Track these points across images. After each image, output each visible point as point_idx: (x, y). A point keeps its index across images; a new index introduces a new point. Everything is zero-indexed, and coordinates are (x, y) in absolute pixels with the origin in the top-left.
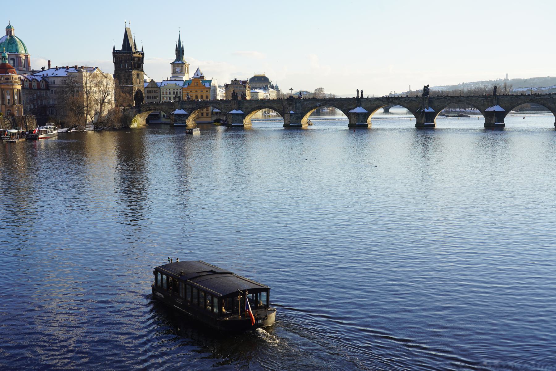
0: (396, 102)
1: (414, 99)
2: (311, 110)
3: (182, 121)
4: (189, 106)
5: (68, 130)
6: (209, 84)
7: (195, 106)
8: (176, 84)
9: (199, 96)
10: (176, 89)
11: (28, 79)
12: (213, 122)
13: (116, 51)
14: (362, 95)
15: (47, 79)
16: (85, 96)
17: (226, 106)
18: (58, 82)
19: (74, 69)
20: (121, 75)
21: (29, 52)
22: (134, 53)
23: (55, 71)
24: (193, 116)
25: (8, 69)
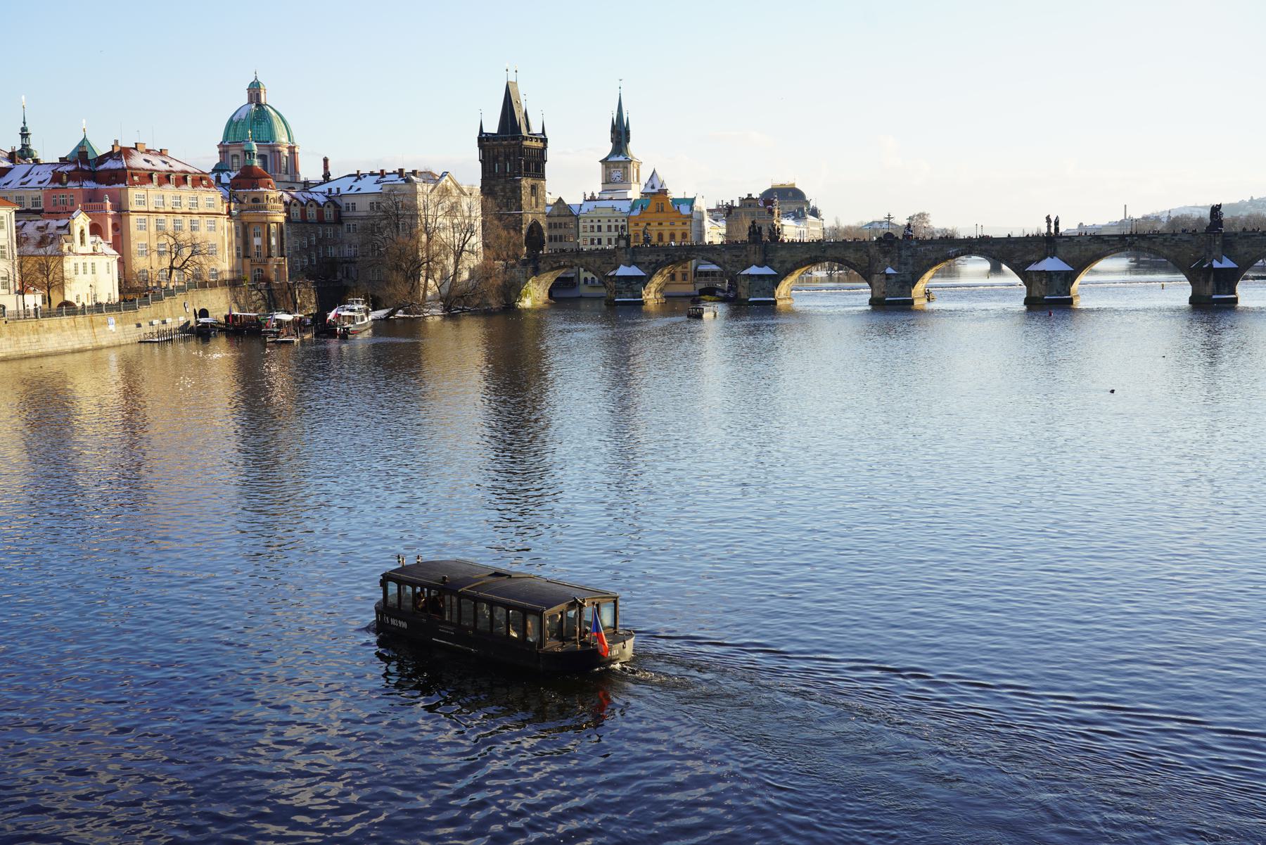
0: (1142, 244)
1: (1185, 237)
2: (936, 264)
3: (633, 291)
4: (650, 257)
6: (688, 207)
7: (662, 258)
8: (614, 209)
10: (613, 220)
11: (297, 199)
12: (698, 293)
13: (486, 134)
14: (1057, 229)
15: (337, 200)
16: (424, 238)
17: (734, 258)
18: (363, 206)
19: (397, 176)
22: (526, 139)
23: (356, 181)
24: (657, 280)
25: (257, 178)
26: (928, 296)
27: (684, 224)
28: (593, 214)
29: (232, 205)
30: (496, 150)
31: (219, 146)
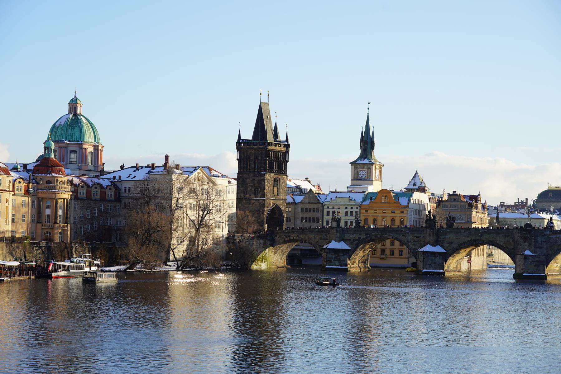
5: (127, 268)
6: (407, 199)
7: (363, 236)
8: (350, 199)
9: (371, 220)
10: (349, 207)
12: (410, 265)
13: (243, 140)
15: (118, 184)
19: (163, 168)
20: (247, 181)
21: (103, 141)
22: (272, 144)
23: (134, 171)
24: (359, 255)
25: (51, 167)
27: (402, 212)
30: (249, 152)
31: (44, 143)
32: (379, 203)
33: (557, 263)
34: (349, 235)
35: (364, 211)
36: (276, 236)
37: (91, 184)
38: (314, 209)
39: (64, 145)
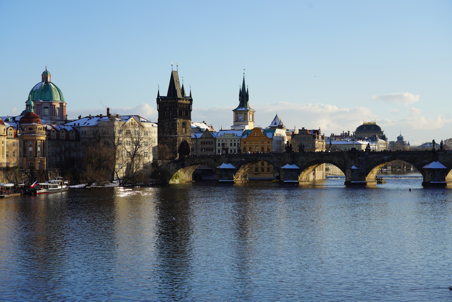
4: (238, 159)
6: (272, 134)
8: (234, 135)
10: (233, 140)
12: (275, 178)
13: (161, 97)
15: (78, 129)
17: (278, 160)
19: (108, 117)
20: (165, 124)
21: (66, 100)
22: (180, 99)
23: (88, 120)
24: (242, 172)
25: (32, 118)
26: (379, 181)
27: (269, 142)
28: (223, 137)
29: (18, 131)
30: (165, 105)
31: (26, 102)
32: (253, 137)
33: (373, 174)
34: (234, 159)
35: (243, 143)
36: (185, 161)
37: (59, 129)
38: (209, 142)
39: (40, 103)
